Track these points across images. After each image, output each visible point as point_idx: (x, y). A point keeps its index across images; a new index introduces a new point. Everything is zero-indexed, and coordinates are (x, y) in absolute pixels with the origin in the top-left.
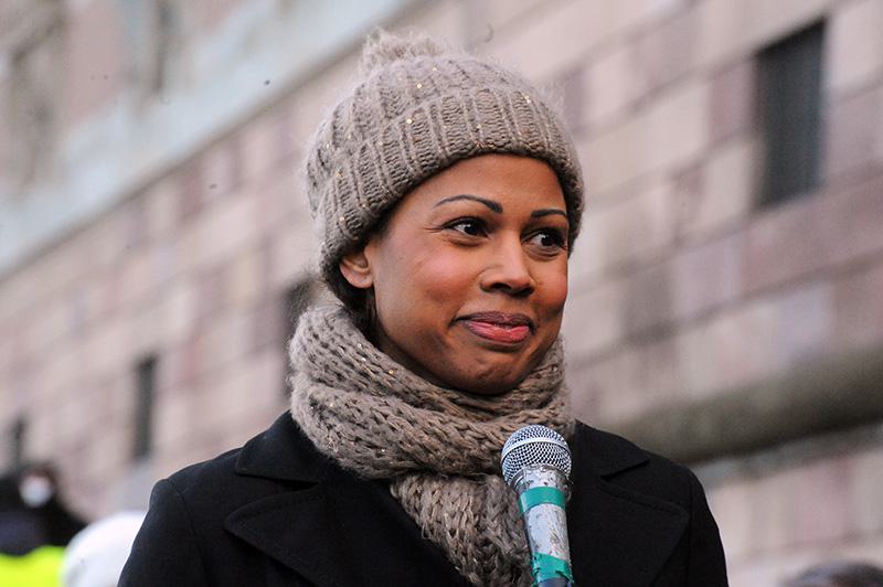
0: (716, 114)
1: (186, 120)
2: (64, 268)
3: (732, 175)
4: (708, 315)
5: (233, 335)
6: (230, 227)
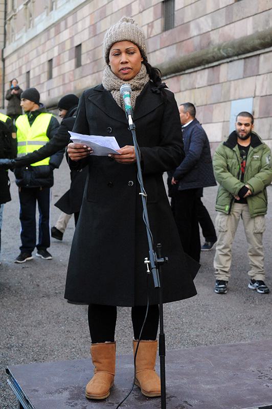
0: (155, 14)
1: (56, 16)
2: (34, 44)
3: (158, 25)
5: (66, 56)
6: (65, 35)
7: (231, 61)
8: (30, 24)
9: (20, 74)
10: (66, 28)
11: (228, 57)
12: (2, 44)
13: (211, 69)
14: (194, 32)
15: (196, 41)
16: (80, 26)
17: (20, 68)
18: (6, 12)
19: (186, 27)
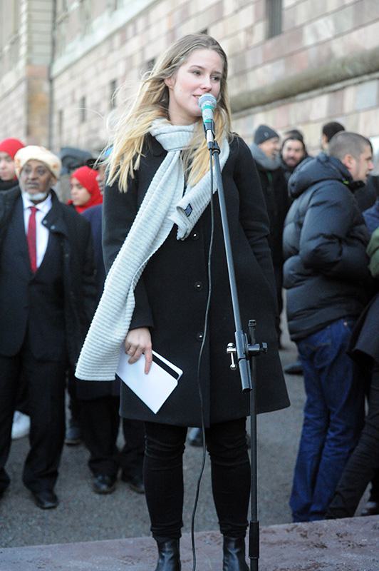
0: (256, 14)
1: (122, 16)
2: (93, 57)
3: (260, 30)
4: (255, 68)
6: (134, 45)
7: (360, 83)
8: (86, 29)
9: (73, 101)
10: (135, 34)
11: (356, 76)
12: (49, 58)
13: (332, 95)
14: (309, 40)
15: (312, 53)
16: (153, 32)
17: (73, 93)
18: (55, 13)
19: (298, 32)
